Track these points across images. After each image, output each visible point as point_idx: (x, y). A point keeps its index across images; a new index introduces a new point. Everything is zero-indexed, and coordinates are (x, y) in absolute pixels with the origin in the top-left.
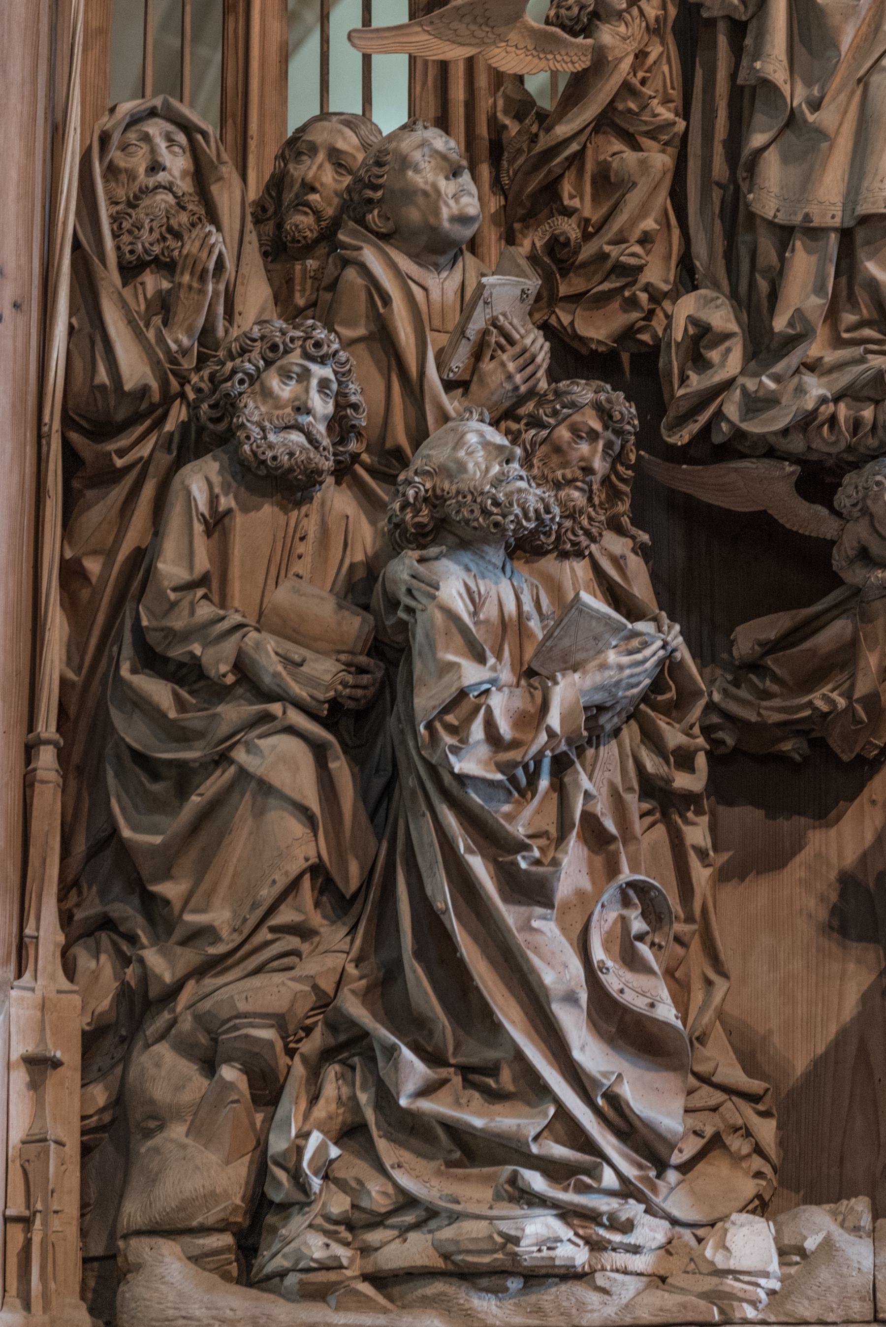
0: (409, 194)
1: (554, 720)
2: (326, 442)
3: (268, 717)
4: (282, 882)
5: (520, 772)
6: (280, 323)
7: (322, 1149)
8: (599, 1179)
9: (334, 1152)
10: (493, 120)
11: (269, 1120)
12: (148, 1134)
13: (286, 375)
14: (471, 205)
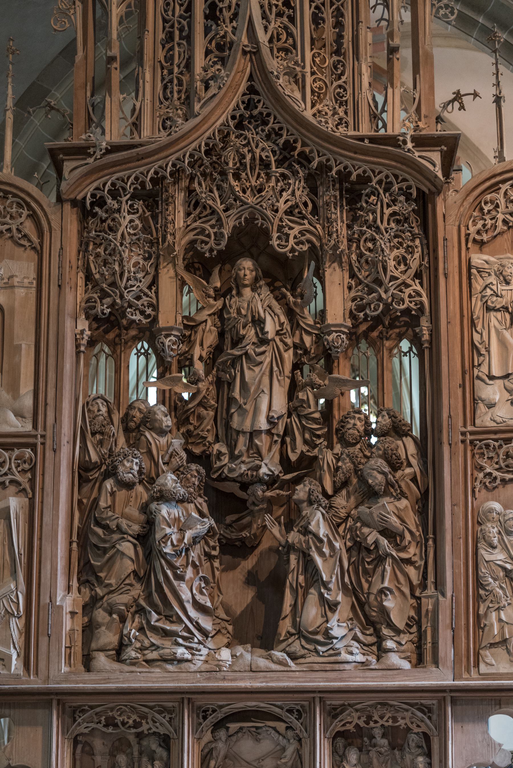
0: (156, 420)
1: (186, 541)
2: (137, 476)
3: (123, 538)
4: (126, 574)
5: (178, 552)
6: (127, 449)
7: (135, 633)
8: (193, 640)
9: (137, 634)
10: (175, 401)
11: (123, 626)
12: (97, 629)
13: (128, 461)
14: (170, 423)
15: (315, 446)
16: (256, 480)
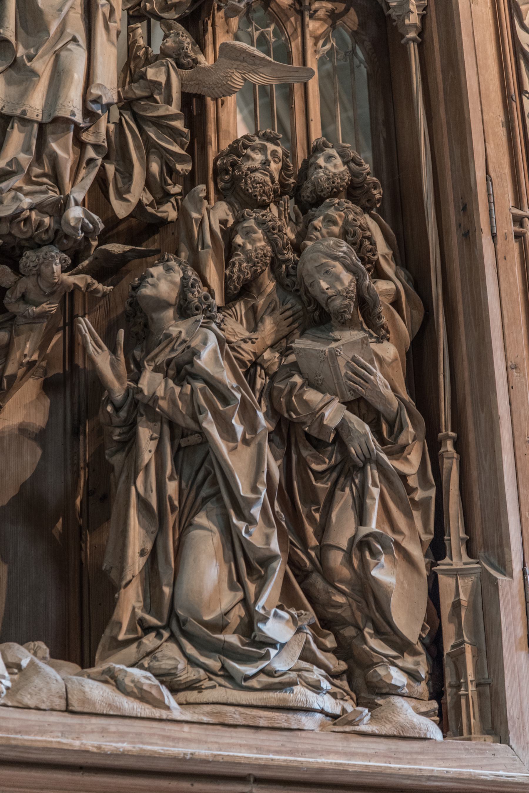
15: (167, 196)
16: (44, 237)
